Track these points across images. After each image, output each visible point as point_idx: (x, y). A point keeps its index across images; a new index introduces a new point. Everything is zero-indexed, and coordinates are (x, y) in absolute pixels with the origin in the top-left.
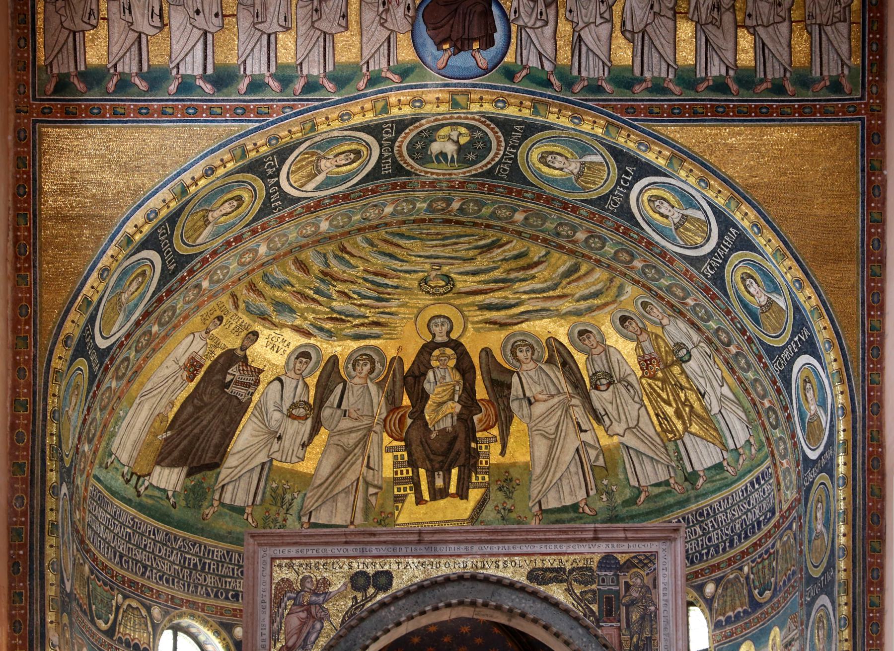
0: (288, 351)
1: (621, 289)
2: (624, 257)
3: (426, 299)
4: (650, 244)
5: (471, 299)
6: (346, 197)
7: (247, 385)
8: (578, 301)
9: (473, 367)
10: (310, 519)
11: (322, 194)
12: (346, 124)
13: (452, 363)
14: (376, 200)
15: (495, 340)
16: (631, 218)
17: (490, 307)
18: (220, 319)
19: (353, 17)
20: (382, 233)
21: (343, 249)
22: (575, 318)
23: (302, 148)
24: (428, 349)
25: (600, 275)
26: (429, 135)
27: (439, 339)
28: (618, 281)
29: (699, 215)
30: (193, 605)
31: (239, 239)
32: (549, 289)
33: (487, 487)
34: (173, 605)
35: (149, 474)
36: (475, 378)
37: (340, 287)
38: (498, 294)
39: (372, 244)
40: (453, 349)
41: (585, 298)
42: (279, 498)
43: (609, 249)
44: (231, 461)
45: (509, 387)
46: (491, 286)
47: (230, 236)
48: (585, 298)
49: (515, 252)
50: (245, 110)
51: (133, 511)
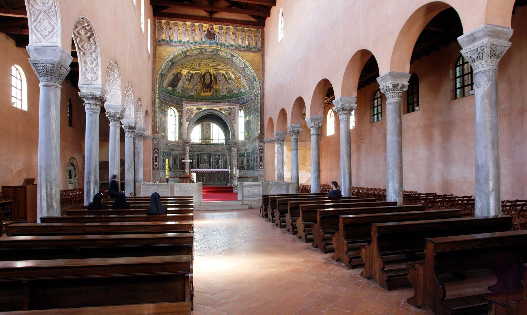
1: (232, 69)
4: (235, 64)
5: (212, 67)
6: (195, 55)
7: (180, 76)
9: (212, 76)
15: (215, 72)
16: (233, 61)
17: (214, 68)
18: (178, 68)
19: (197, 35)
20: (200, 59)
22: (225, 71)
25: (229, 67)
28: (231, 68)
30: (173, 105)
31: (181, 60)
34: (170, 106)
35: (167, 88)
39: (198, 60)
42: (184, 91)
43: (230, 64)
45: (217, 78)
47: (180, 60)
50: (183, 46)
51: (165, 93)
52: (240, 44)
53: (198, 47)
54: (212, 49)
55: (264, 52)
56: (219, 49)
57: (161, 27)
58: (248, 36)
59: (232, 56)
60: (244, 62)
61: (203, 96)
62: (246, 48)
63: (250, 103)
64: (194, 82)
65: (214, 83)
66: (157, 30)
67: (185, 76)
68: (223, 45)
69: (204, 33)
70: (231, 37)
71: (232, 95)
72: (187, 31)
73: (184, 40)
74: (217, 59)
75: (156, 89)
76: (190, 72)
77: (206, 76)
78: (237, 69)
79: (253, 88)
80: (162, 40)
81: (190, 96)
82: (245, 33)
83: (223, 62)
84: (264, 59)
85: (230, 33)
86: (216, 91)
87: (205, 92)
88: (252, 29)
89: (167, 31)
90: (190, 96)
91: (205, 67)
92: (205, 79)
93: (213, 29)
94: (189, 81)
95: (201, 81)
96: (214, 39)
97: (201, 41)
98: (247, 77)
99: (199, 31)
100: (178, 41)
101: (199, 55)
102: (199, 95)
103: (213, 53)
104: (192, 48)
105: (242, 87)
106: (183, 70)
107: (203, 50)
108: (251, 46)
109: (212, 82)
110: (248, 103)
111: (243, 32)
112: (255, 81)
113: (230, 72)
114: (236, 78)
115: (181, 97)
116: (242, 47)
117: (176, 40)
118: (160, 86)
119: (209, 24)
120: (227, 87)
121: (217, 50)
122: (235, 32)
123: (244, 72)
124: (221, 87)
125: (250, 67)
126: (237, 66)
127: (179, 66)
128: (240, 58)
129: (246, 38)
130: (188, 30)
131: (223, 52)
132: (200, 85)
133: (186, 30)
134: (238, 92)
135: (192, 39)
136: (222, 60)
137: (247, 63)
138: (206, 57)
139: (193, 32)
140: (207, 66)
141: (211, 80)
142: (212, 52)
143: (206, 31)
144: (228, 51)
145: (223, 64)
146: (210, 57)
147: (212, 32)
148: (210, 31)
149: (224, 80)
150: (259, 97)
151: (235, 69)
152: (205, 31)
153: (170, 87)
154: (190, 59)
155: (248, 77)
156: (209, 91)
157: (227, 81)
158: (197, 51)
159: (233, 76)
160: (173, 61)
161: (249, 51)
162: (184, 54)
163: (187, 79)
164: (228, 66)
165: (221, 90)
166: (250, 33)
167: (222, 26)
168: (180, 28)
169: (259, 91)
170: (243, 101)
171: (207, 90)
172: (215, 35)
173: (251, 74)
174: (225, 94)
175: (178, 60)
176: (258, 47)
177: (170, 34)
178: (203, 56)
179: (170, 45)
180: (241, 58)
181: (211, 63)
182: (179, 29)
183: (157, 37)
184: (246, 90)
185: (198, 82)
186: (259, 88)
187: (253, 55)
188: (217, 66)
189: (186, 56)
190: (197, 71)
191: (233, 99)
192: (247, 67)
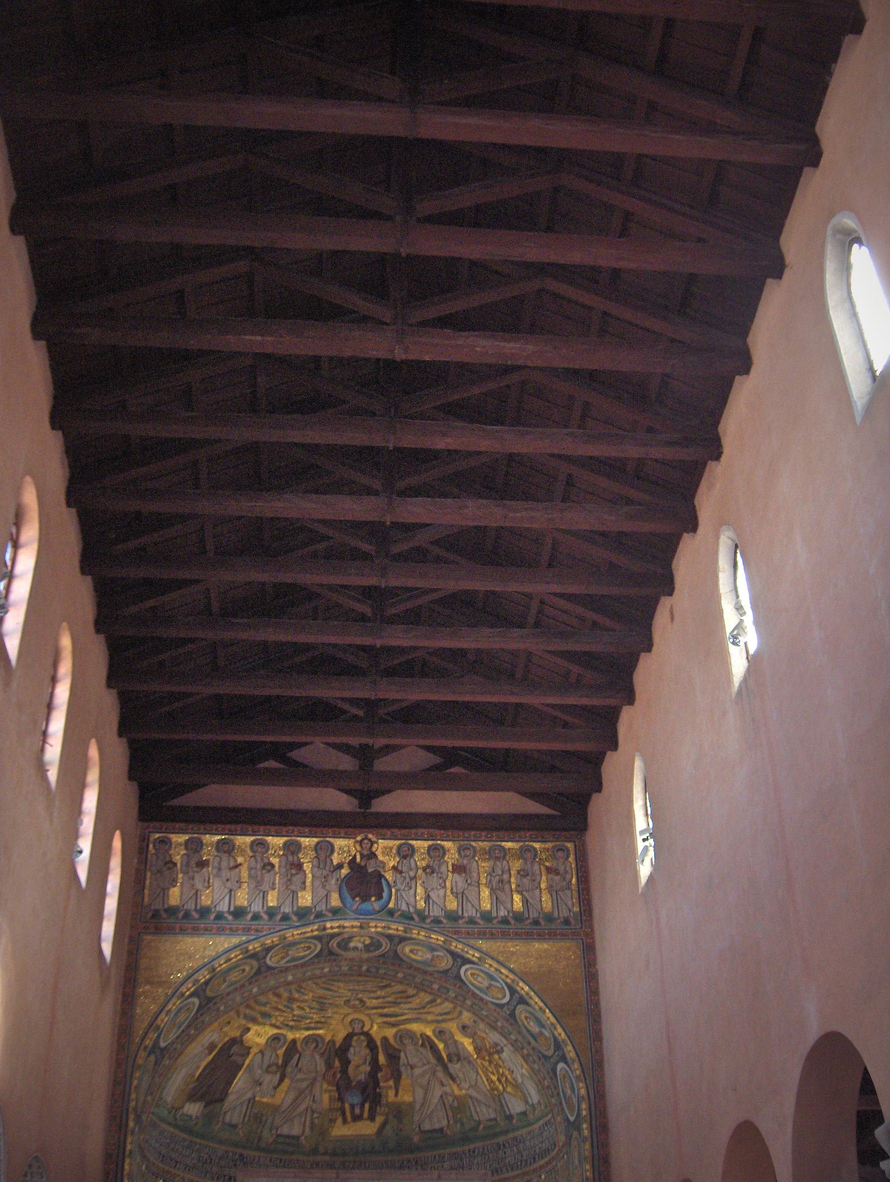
0: (267, 1037)
1: (460, 1013)
2: (461, 998)
3: (350, 1011)
4: (474, 994)
5: (375, 1011)
6: (303, 965)
8: (437, 1015)
9: (377, 1047)
10: (277, 1132)
11: (289, 965)
12: (302, 936)
13: (365, 1044)
14: (321, 966)
15: (390, 1033)
16: (462, 981)
17: (386, 1015)
20: (323, 979)
21: (301, 987)
23: (280, 946)
24: (349, 1037)
25: (448, 1006)
26: (350, 938)
27: (356, 1031)
28: (459, 1009)
29: (498, 985)
31: (243, 986)
32: (419, 1009)
33: (387, 1115)
36: (378, 1053)
37: (298, 1004)
38: (392, 1009)
39: (317, 984)
40: (365, 1036)
41: (441, 1014)
43: (452, 994)
44: (231, 1098)
45: (399, 1058)
46: (386, 1005)
47: (238, 985)
48: (441, 1014)
49: (399, 990)
52: (488, 907)
53: (312, 931)
54: (371, 938)
55: (590, 935)
56: (398, 936)
57: (168, 859)
58: (518, 872)
59: (454, 960)
60: (509, 981)
61: (343, 1139)
62: (512, 922)
63: (547, 1163)
64: (300, 1076)
65: (386, 1081)
66: (149, 874)
67: (261, 1052)
68: (415, 916)
69: (336, 875)
70: (448, 884)
71: (467, 1127)
72: (269, 871)
73: (257, 907)
74: (395, 976)
75: (127, 1114)
76: (285, 1036)
77: (352, 1050)
78: (484, 1013)
79: (555, 1094)
80: (166, 910)
81: (281, 1140)
82: (505, 863)
83: (420, 988)
84: (594, 966)
85: (443, 869)
86: (399, 1112)
87: (349, 1118)
88: (537, 845)
89: (191, 874)
90: (281, 1140)
91: (346, 1012)
92: (349, 1062)
93: (375, 856)
94: (278, 1075)
95: (332, 1071)
96: (380, 897)
97: (324, 907)
98: (525, 1045)
99: (316, 869)
100: (229, 912)
101: (318, 963)
102: (324, 1133)
103: (377, 953)
104: (285, 938)
105: (509, 1089)
106: (254, 1028)
107: (334, 943)
108: (534, 915)
109: (379, 1075)
110: (542, 1162)
111: (497, 858)
112: (564, 1059)
113: (453, 1027)
114: (484, 1053)
115: (244, 1147)
116: (495, 921)
117: (224, 907)
118: (149, 1098)
119: (359, 838)
120: (446, 1093)
121: (390, 937)
122: (465, 862)
123: (511, 1024)
124: (420, 1093)
125: (537, 1000)
126: (482, 1000)
127: (232, 1013)
128: (490, 966)
129: (510, 882)
130: (273, 866)
131: (418, 944)
132: (326, 1091)
133: (263, 868)
134: (493, 1116)
135: (288, 902)
136: (418, 980)
137: (521, 984)
138: (350, 969)
139: (292, 875)
140: (354, 1007)
141: (375, 1067)
142: (372, 948)
143: (346, 865)
144: (438, 938)
145: (422, 994)
146: (364, 968)
147: (370, 870)
148: (359, 866)
149: (429, 1063)
150: (586, 1133)
151: (474, 1013)
152: (340, 866)
153: (195, 1101)
154: (282, 980)
155: (529, 1044)
156: (366, 1115)
157: (445, 1068)
158: (309, 948)
159: (467, 1043)
160: (209, 993)
161: (528, 936)
162: (255, 964)
163: (269, 1066)
164: (440, 1004)
165: (418, 1107)
166: (525, 859)
167: (413, 842)
168: (240, 860)
169: (584, 1106)
170: (519, 1152)
171: (357, 1111)
172: (383, 881)
173: (543, 1030)
174: (437, 1126)
175: (232, 988)
176: (565, 913)
177: (199, 885)
178: (336, 969)
179: (195, 931)
180: (495, 965)
181: (372, 995)
182: (238, 866)
183: (146, 900)
184: (527, 1102)
185: (320, 1079)
186: (583, 1092)
187: (546, 950)
188: (399, 1003)
189: (263, 969)
190: (311, 1032)
191: (472, 1146)
192: (522, 1001)
